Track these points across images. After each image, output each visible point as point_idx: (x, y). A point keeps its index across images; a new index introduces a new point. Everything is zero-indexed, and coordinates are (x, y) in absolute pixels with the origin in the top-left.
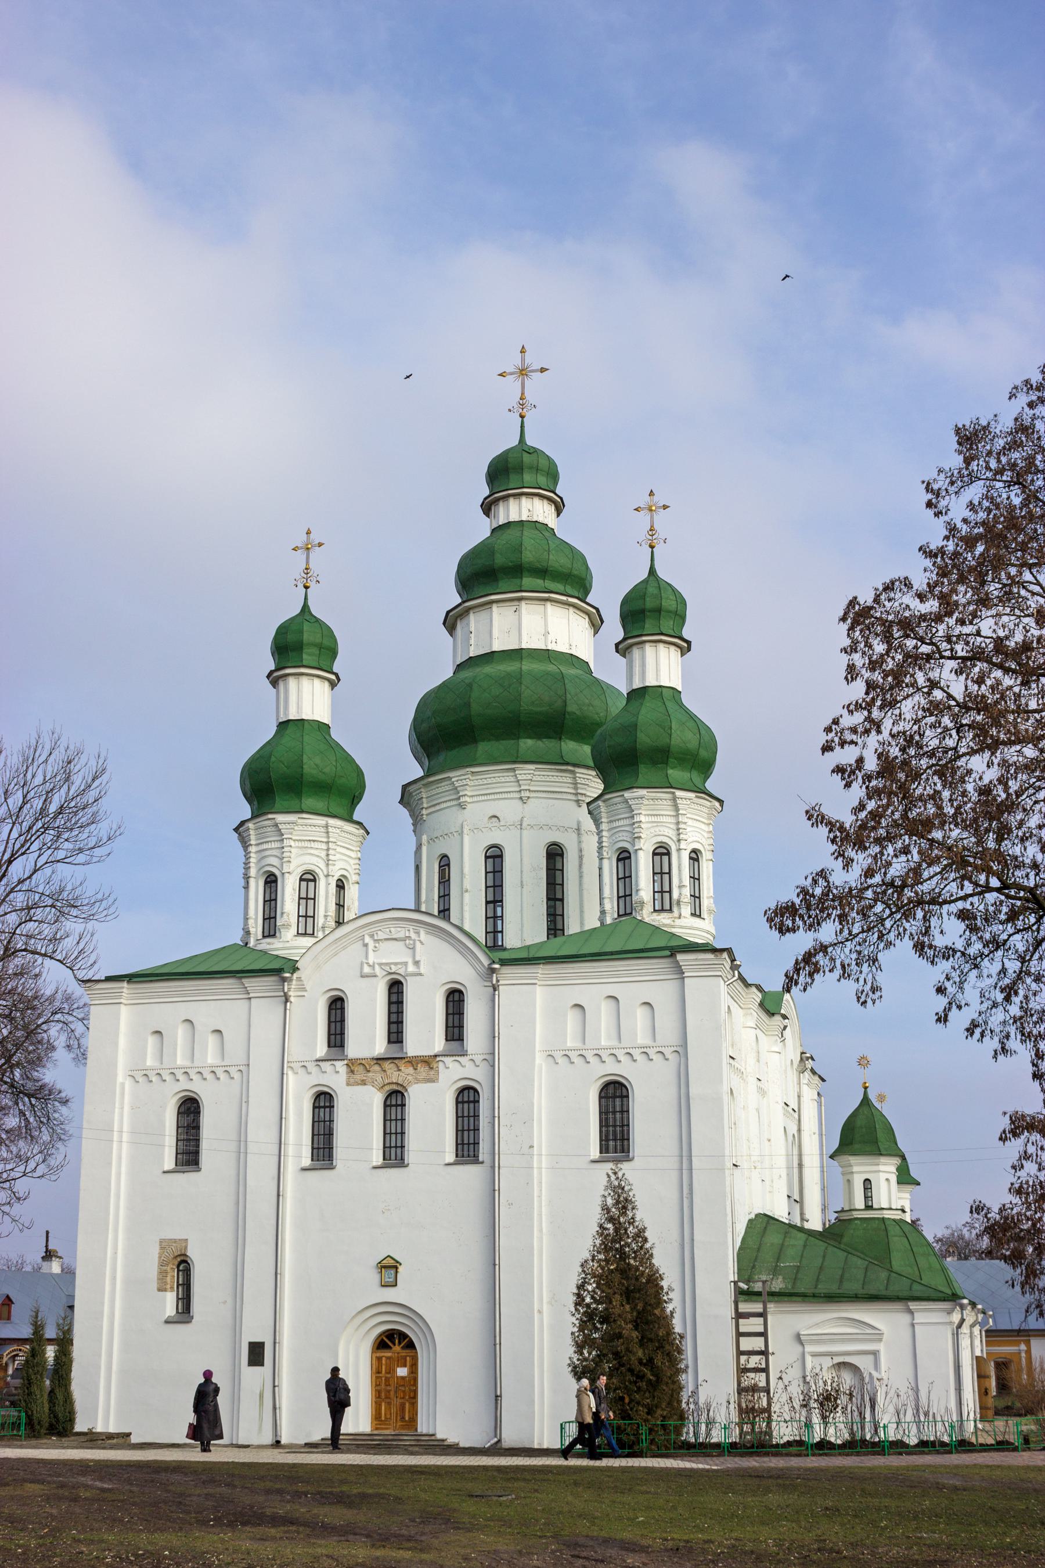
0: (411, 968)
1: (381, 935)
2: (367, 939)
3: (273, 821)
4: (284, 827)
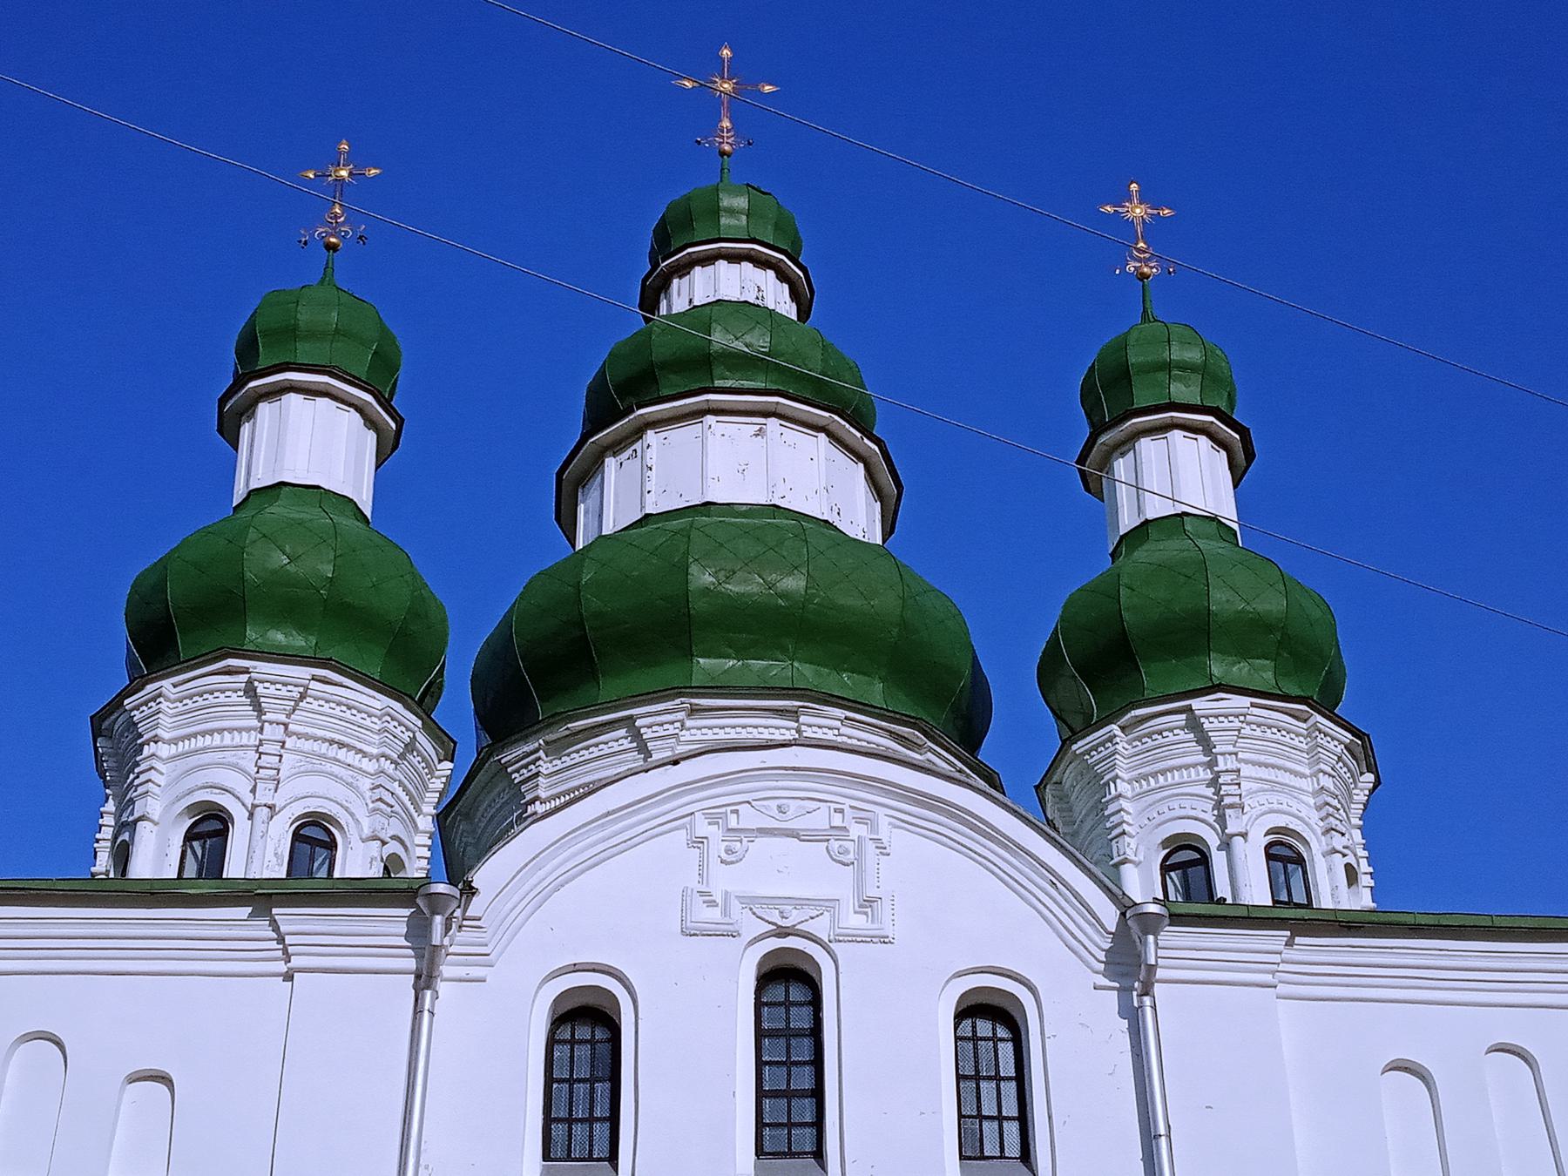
0: (855, 922)
1: (749, 818)
2: (703, 828)
3: (245, 678)
4: (272, 690)
